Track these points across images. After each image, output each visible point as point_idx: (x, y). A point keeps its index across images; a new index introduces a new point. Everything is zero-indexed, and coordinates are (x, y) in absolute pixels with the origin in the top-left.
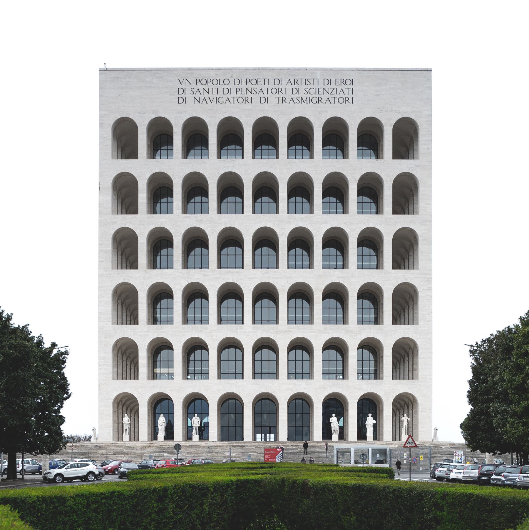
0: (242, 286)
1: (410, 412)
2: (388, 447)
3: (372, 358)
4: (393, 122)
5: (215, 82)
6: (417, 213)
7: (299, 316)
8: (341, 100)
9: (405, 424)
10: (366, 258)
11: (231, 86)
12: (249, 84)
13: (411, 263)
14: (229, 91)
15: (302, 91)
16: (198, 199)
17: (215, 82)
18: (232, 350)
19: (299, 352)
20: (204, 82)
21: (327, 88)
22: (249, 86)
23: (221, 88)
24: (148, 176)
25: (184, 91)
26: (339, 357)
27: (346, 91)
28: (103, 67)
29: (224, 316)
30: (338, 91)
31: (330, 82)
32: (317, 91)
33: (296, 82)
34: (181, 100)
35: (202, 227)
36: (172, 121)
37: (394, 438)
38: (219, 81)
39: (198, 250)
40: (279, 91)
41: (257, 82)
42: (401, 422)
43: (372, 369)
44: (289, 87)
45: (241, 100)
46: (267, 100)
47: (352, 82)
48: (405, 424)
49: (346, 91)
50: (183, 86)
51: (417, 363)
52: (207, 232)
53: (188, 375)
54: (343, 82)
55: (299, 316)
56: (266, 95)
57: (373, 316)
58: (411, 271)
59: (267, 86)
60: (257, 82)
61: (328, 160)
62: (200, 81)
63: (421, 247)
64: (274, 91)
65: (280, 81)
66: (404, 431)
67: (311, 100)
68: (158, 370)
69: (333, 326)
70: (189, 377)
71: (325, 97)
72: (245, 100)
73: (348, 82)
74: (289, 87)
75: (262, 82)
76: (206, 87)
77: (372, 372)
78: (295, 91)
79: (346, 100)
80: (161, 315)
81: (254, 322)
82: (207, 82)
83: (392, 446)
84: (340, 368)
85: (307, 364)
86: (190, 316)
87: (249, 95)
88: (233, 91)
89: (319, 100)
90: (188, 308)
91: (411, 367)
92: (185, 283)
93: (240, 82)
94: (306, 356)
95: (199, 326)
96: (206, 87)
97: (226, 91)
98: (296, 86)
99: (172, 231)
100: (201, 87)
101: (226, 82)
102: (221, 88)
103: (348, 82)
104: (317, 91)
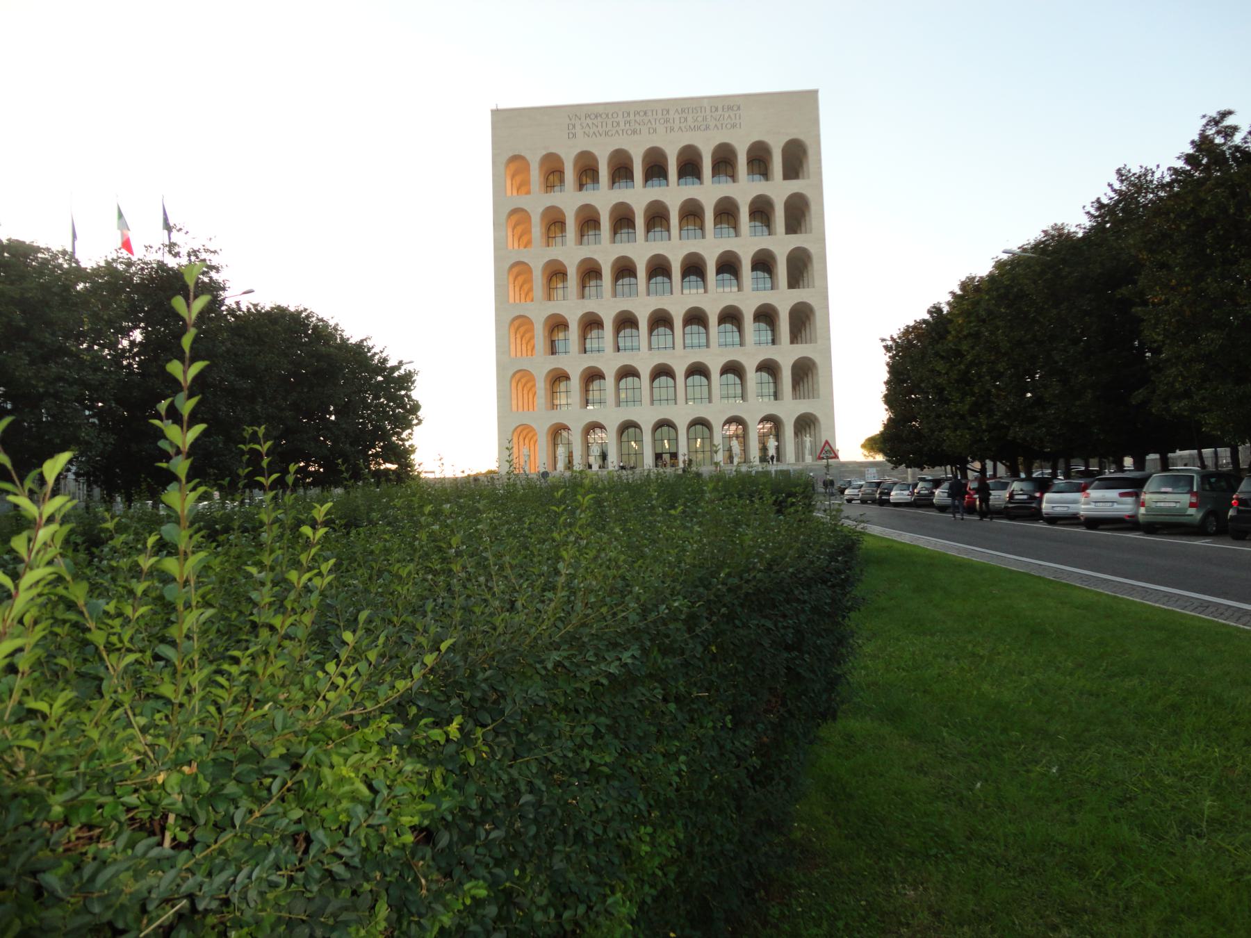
0: (637, 314)
1: (813, 432)
2: (791, 468)
3: (771, 380)
4: (782, 144)
5: (604, 116)
6: (811, 232)
7: (696, 341)
8: (729, 126)
9: (808, 444)
10: (761, 281)
11: (620, 119)
12: (637, 116)
13: (806, 281)
14: (618, 124)
15: (690, 119)
17: (604, 116)
18: (630, 379)
19: (697, 378)
20: (593, 117)
21: (714, 115)
22: (638, 118)
23: (609, 123)
24: (541, 210)
25: (574, 126)
26: (738, 381)
27: (733, 117)
28: (494, 108)
29: (621, 345)
30: (726, 117)
31: (717, 109)
32: (705, 119)
33: (683, 111)
34: (571, 136)
35: (595, 257)
36: (563, 156)
37: (797, 459)
38: (607, 115)
39: (593, 283)
40: (667, 121)
41: (645, 113)
42: (803, 443)
43: (772, 390)
44: (677, 116)
45: (629, 132)
46: (655, 131)
47: (739, 108)
48: (808, 444)
49: (733, 117)
50: (573, 122)
51: (818, 383)
52: (601, 262)
53: (587, 403)
54: (730, 108)
55: (696, 341)
56: (654, 126)
57: (770, 338)
58: (806, 290)
59: (655, 116)
60: (645, 113)
61: (717, 185)
62: (589, 116)
63: (816, 264)
64: (662, 121)
65: (668, 112)
66: (807, 452)
67: (699, 128)
68: (557, 402)
69: (730, 348)
70: (591, 407)
71: (712, 124)
72: (634, 132)
73: (735, 108)
74: (677, 116)
75: (650, 113)
76: (595, 122)
77: (772, 393)
78: (682, 120)
79: (734, 126)
80: (560, 346)
81: (650, 348)
82: (596, 117)
83: (796, 467)
84: (739, 391)
85: (705, 389)
86: (588, 346)
87: (638, 127)
88: (622, 124)
89: (707, 128)
90: (585, 339)
91: (810, 388)
92: (580, 313)
93: (629, 114)
94: (704, 380)
95: (595, 355)
96: (595, 122)
97: (615, 124)
98: (684, 115)
99: (566, 263)
100: (589, 121)
101: (615, 115)
102: (609, 123)
103: (735, 108)
104: (705, 119)
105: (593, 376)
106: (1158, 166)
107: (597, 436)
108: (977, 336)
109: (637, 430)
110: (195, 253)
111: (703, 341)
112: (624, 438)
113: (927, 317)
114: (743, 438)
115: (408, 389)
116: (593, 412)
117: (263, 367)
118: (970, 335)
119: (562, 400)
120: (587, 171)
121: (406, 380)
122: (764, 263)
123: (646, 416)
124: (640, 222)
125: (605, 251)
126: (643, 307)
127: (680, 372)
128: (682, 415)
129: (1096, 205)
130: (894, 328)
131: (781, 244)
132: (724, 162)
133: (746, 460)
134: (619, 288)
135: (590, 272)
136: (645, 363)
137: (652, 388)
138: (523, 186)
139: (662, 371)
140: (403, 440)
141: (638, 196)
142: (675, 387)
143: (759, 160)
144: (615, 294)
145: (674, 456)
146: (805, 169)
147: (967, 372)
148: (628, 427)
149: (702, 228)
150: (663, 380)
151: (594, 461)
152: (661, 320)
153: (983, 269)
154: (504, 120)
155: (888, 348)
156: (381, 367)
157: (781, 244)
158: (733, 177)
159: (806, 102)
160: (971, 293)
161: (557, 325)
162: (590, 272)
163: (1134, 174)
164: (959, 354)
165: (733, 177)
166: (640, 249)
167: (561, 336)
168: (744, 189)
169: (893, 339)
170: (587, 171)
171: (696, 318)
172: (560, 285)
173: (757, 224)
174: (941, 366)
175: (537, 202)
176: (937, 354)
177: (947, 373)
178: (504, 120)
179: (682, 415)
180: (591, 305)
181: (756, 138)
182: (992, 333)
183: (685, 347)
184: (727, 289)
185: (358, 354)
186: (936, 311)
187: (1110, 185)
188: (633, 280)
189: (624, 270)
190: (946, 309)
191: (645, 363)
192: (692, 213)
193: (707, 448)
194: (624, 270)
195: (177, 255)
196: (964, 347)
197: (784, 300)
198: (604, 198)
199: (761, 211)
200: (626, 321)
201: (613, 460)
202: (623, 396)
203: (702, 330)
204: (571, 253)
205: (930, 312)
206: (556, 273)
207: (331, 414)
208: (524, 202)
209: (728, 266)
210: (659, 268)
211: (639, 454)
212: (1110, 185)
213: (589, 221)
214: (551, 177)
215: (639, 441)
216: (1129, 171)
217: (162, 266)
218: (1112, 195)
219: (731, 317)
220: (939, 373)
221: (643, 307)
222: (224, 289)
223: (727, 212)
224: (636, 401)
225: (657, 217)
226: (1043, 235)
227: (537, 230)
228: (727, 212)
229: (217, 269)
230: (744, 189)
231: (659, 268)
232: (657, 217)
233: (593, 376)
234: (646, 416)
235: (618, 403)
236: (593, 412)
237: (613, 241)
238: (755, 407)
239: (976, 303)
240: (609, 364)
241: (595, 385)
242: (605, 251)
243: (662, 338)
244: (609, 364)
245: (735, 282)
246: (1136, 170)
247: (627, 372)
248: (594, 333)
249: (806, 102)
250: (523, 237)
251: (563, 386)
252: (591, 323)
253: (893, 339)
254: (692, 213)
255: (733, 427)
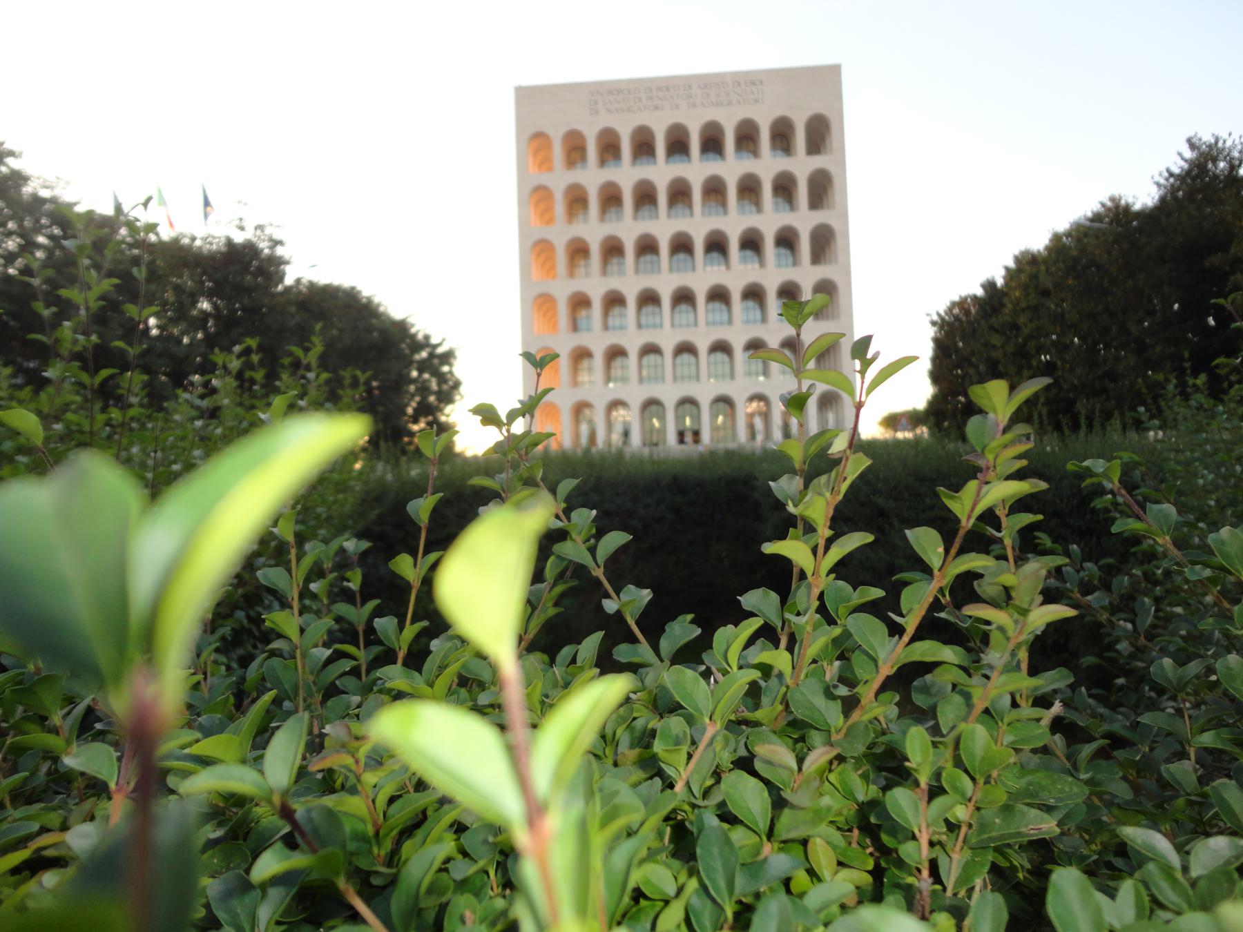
14: (640, 100)
16: (613, 209)
25: (596, 103)
29: (643, 321)
31: (739, 84)
33: (706, 86)
39: (615, 261)
46: (677, 106)
47: (761, 83)
53: (608, 379)
54: (753, 83)
60: (668, 89)
65: (690, 87)
70: (611, 385)
72: (656, 108)
79: (756, 101)
80: (582, 324)
81: (673, 325)
89: (730, 103)
94: (726, 358)
105: (615, 353)
106: (1230, 134)
107: (620, 414)
108: (1035, 309)
109: (660, 408)
110: (260, 227)
111: (725, 317)
112: (647, 414)
113: (980, 292)
114: (766, 416)
115: (450, 365)
116: (614, 390)
117: (1106, 256)
118: (1028, 307)
119: (584, 377)
120: (609, 148)
121: (448, 357)
122: (786, 240)
123: (669, 394)
124: (662, 199)
125: (628, 228)
126: (666, 285)
127: (703, 346)
128: (705, 391)
129: (1166, 174)
130: (940, 304)
131: (804, 221)
132: (747, 137)
133: (768, 435)
134: (641, 266)
135: (613, 249)
136: (668, 340)
137: (674, 365)
138: (545, 163)
139: (686, 349)
140: (448, 416)
141: (661, 173)
142: (697, 364)
143: (782, 136)
144: (637, 271)
145: (696, 434)
146: (827, 143)
147: (1025, 345)
148: (651, 405)
149: (724, 204)
150: (686, 357)
151: (616, 438)
152: (684, 297)
153: (1039, 243)
154: (528, 97)
155: (934, 323)
156: (426, 343)
157: (804, 221)
158: (755, 153)
159: (829, 76)
160: (1027, 266)
161: (580, 302)
162: (613, 249)
163: (1205, 143)
164: (1015, 327)
165: (755, 153)
166: (663, 227)
167: (583, 313)
168: (767, 165)
169: (939, 315)
170: (609, 148)
171: (719, 295)
172: (582, 263)
173: (780, 200)
174: (996, 340)
175: (559, 180)
176: (991, 328)
177: (1002, 347)
178: (528, 97)
179: (705, 391)
180: (614, 283)
181: (778, 112)
182: (1057, 305)
183: (708, 324)
184: (749, 266)
185: (402, 327)
186: (990, 286)
187: (1180, 154)
188: (655, 258)
189: (647, 247)
190: (1000, 282)
191: (668, 340)
192: (714, 189)
193: (729, 424)
194: (647, 247)
195: (242, 228)
196: (1022, 320)
197: (806, 276)
198: (627, 175)
199: (784, 188)
200: (649, 299)
201: (636, 439)
202: (645, 373)
203: (724, 307)
204: (593, 230)
205: (984, 286)
206: (579, 250)
207: (378, 388)
208: (545, 179)
209: (751, 243)
210: (682, 245)
211: (663, 431)
212: (1180, 154)
213: (611, 198)
214: (573, 155)
215: (662, 418)
216: (1200, 140)
217: (230, 243)
218: (1183, 164)
219: (754, 294)
220: (994, 347)
221: (666, 285)
222: (287, 263)
223: (749, 188)
224: (659, 378)
225: (680, 194)
226: (1099, 206)
227: (560, 207)
228: (749, 188)
229: (280, 243)
230: (767, 165)
231: (682, 245)
232: (680, 194)
233: (615, 353)
234: (669, 394)
235: (641, 380)
236: (614, 390)
237: (635, 218)
238: (780, 383)
239: (1034, 277)
240: (632, 341)
241: (618, 362)
242: (628, 228)
243: (684, 316)
244: (632, 341)
245: (756, 258)
246: (1207, 138)
247: (651, 350)
248: (616, 311)
249: (829, 76)
250: (546, 214)
251: (585, 363)
252: (614, 300)
253: (939, 315)
254: (714, 189)
255: (754, 405)
